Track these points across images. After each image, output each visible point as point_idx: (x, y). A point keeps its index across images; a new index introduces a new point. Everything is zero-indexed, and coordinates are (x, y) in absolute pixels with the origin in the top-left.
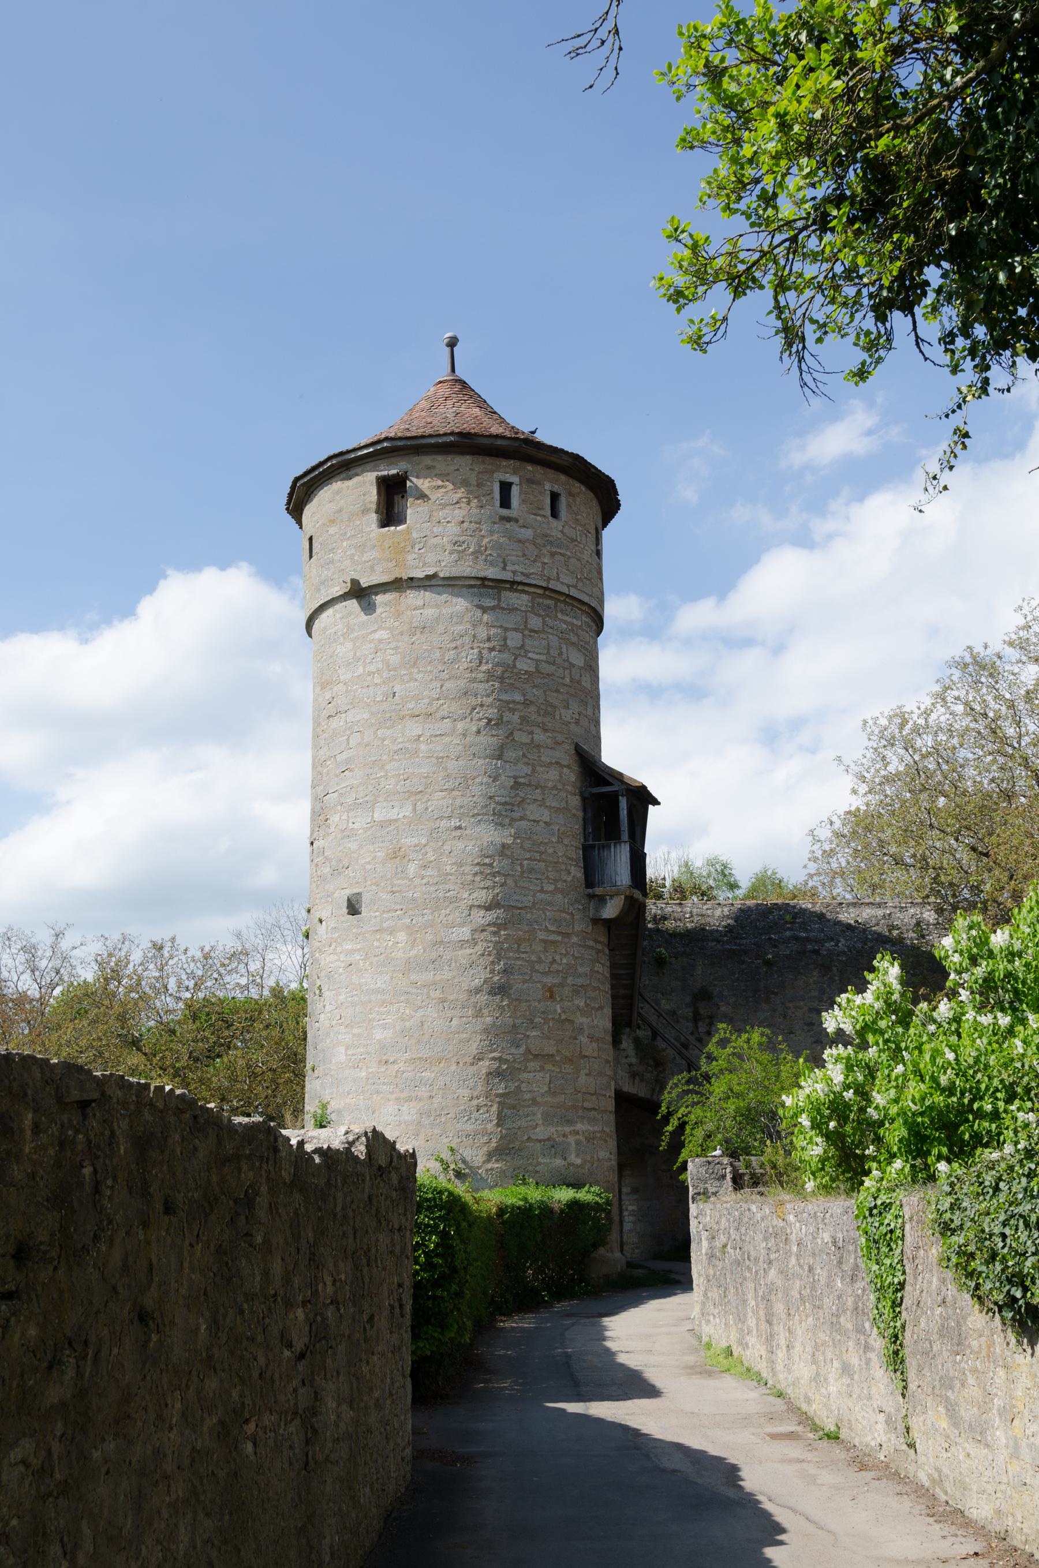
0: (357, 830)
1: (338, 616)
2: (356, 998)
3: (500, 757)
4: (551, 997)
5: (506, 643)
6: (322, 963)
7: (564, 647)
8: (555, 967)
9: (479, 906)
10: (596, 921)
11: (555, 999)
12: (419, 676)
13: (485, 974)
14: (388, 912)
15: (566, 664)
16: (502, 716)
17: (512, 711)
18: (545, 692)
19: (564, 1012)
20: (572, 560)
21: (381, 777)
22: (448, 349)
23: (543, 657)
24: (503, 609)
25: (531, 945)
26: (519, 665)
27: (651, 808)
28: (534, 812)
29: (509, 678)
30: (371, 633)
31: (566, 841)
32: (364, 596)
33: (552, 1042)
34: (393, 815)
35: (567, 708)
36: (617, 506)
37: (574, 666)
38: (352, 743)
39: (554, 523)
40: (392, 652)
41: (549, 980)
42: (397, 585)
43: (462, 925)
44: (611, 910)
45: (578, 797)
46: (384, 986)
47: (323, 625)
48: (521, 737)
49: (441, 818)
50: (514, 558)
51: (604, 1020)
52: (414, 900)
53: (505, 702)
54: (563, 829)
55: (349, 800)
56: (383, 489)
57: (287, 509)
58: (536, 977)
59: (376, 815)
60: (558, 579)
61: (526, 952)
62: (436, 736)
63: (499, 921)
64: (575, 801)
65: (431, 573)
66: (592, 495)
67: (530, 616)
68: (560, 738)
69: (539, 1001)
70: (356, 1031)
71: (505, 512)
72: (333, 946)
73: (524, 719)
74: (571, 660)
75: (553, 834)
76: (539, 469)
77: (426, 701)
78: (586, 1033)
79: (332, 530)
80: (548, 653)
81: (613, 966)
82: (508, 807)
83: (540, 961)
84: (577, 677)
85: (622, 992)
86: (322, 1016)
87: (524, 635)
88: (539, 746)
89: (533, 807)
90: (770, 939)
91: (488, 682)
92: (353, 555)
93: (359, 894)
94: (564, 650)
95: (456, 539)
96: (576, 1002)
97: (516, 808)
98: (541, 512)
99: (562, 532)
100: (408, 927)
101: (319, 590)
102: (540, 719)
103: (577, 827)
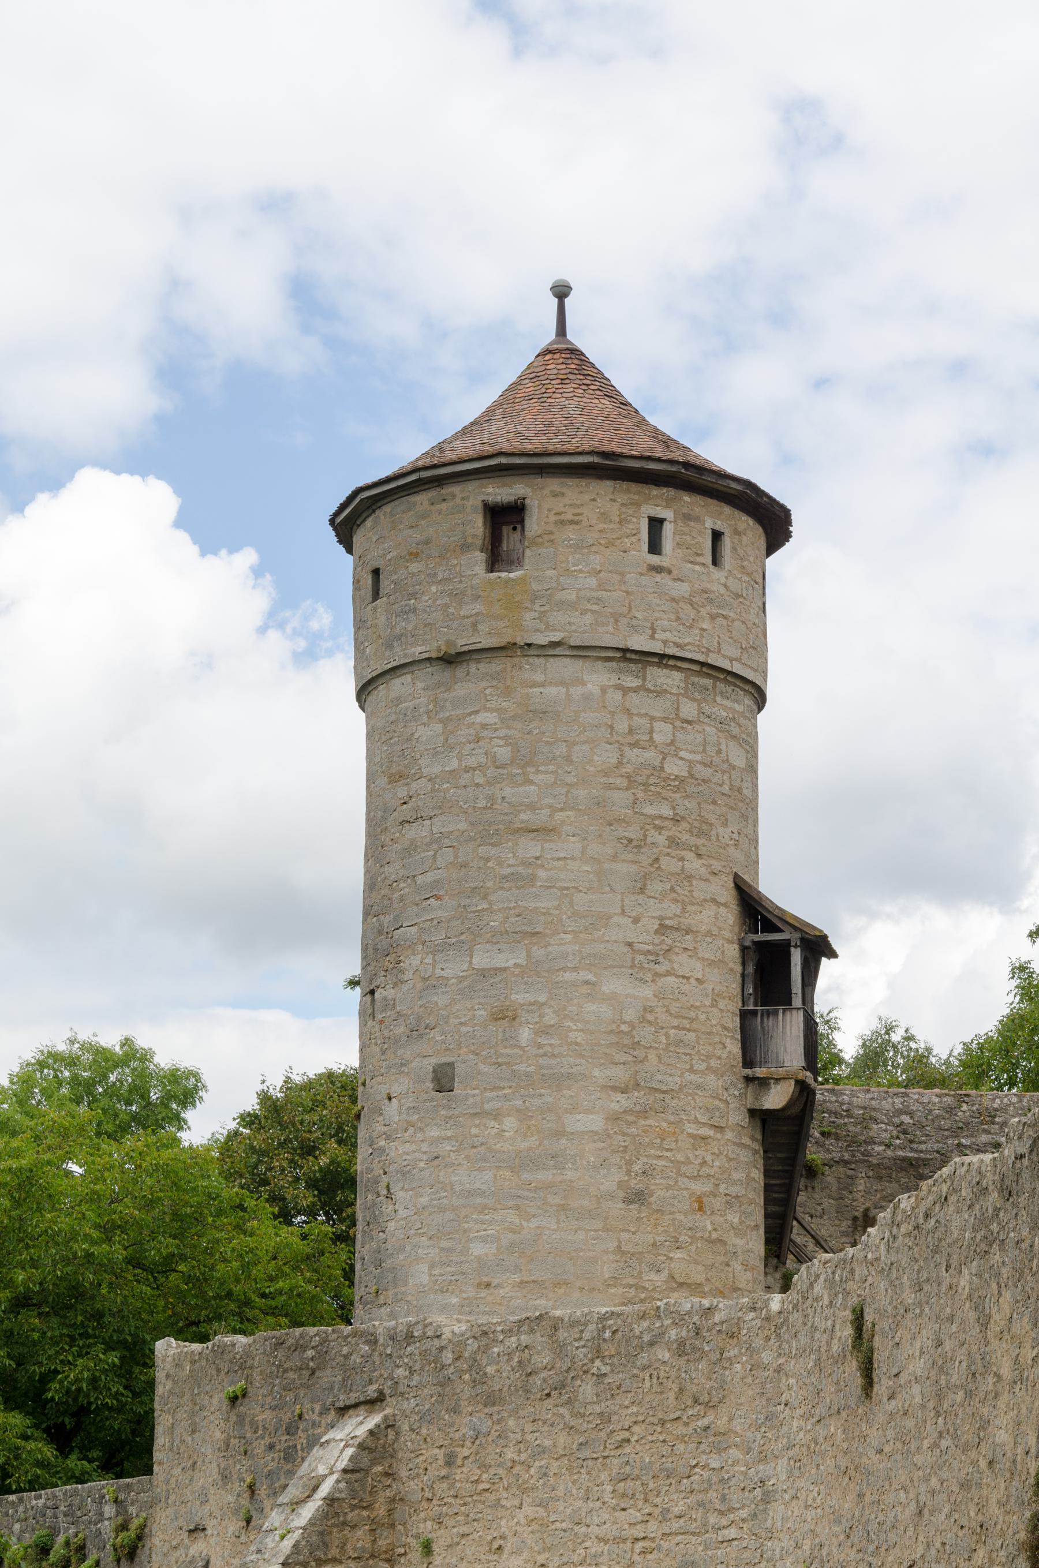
0: (448, 979)
1: (420, 685)
2: (445, 1201)
3: (642, 890)
4: (700, 1209)
5: (651, 738)
6: (393, 1154)
7: (723, 741)
8: (706, 1170)
9: (614, 1088)
10: (753, 1113)
11: (705, 1212)
12: (538, 778)
13: (618, 1176)
14: (491, 1090)
15: (726, 766)
16: (645, 836)
17: (659, 829)
18: (699, 804)
19: (715, 1229)
20: (738, 624)
21: (483, 910)
22: (556, 300)
23: (698, 757)
24: (648, 691)
25: (677, 1141)
26: (668, 769)
27: (824, 961)
28: (683, 963)
29: (656, 785)
30: (470, 714)
31: (722, 1004)
32: (461, 662)
33: (700, 1268)
34: (502, 960)
35: (725, 824)
36: (787, 536)
37: (734, 767)
38: (440, 862)
39: (717, 574)
40: (502, 743)
41: (698, 1187)
42: (507, 649)
43: (588, 1111)
44: (776, 1098)
45: (736, 946)
46: (484, 1187)
47: (393, 695)
48: (669, 864)
49: (564, 969)
50: (665, 623)
51: (756, 1244)
52: (527, 1075)
53: (650, 817)
54: (718, 988)
55: (438, 937)
56: (488, 516)
57: (332, 522)
58: (683, 1182)
59: (474, 961)
60: (719, 652)
61: (671, 1150)
62: (559, 859)
63: (638, 1108)
64: (733, 952)
65: (556, 639)
66: (761, 529)
67: (683, 700)
68: (717, 865)
69: (685, 1214)
70: (444, 1244)
71: (654, 559)
72: (411, 1130)
73: (673, 842)
74: (732, 760)
75: (706, 995)
76: (699, 499)
77: (547, 811)
78: (740, 1258)
79: (414, 567)
80: (704, 751)
81: (767, 1173)
82: (651, 958)
83: (688, 1162)
84: (737, 783)
85: (773, 1208)
86: (392, 1225)
87: (674, 727)
88: (689, 878)
89: (683, 958)
90: (959, 1145)
91: (627, 789)
92: (447, 606)
93: (451, 1065)
94: (723, 747)
95: (588, 594)
96: (730, 1217)
97: (661, 959)
98: (699, 559)
99: (725, 586)
100: (518, 1111)
101: (390, 647)
102: (693, 841)
103: (735, 987)
